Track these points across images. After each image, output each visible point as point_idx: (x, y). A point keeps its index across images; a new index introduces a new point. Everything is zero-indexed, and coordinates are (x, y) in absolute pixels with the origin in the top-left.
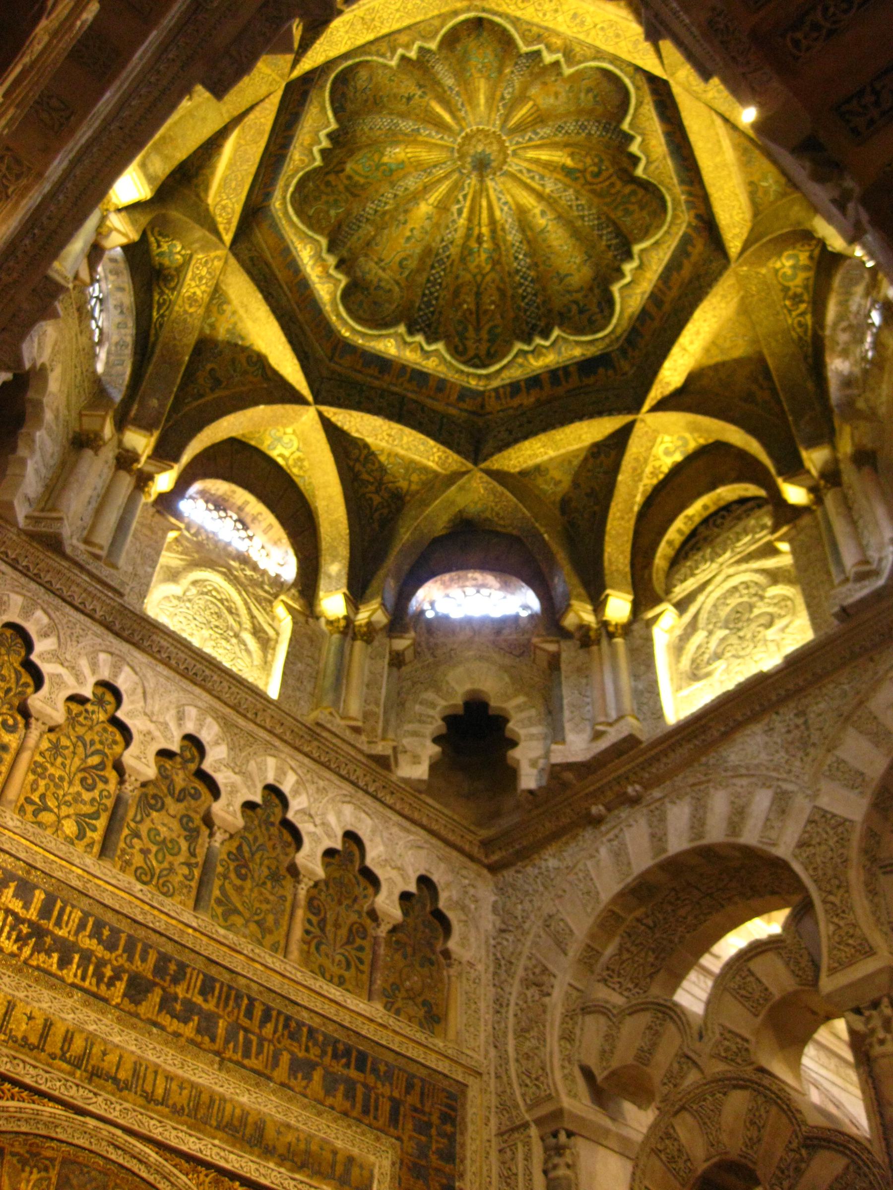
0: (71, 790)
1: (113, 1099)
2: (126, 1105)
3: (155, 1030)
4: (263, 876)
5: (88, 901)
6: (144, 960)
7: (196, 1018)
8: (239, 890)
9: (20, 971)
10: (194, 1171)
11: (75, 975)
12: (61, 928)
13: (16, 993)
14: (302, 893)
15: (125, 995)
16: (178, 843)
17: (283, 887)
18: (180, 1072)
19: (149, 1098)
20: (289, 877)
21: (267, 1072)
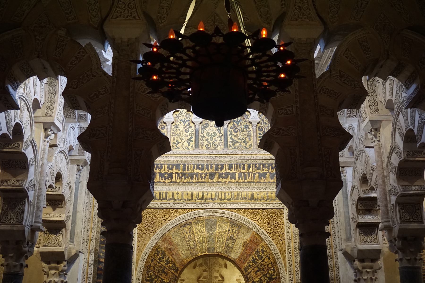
0: (184, 135)
1: (212, 203)
2: (216, 203)
3: (219, 183)
4: (242, 129)
5: (193, 161)
6: (211, 168)
7: (229, 176)
8: (236, 136)
9: (183, 185)
10: (238, 211)
11: (196, 180)
12: (189, 171)
13: (183, 190)
14: (255, 128)
15: (209, 179)
16: (215, 133)
17: (249, 128)
18: (228, 191)
19: (221, 200)
20: (250, 124)
21: (253, 181)
